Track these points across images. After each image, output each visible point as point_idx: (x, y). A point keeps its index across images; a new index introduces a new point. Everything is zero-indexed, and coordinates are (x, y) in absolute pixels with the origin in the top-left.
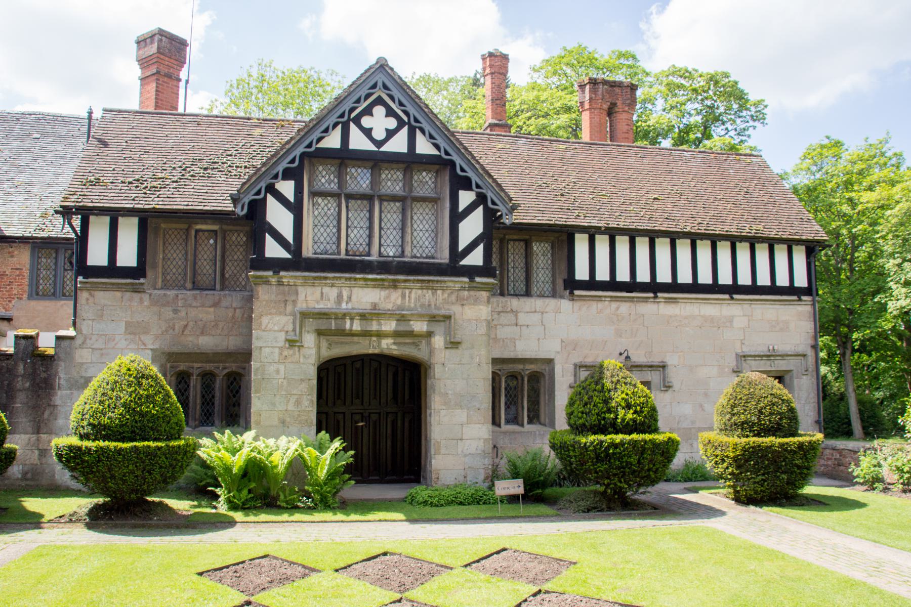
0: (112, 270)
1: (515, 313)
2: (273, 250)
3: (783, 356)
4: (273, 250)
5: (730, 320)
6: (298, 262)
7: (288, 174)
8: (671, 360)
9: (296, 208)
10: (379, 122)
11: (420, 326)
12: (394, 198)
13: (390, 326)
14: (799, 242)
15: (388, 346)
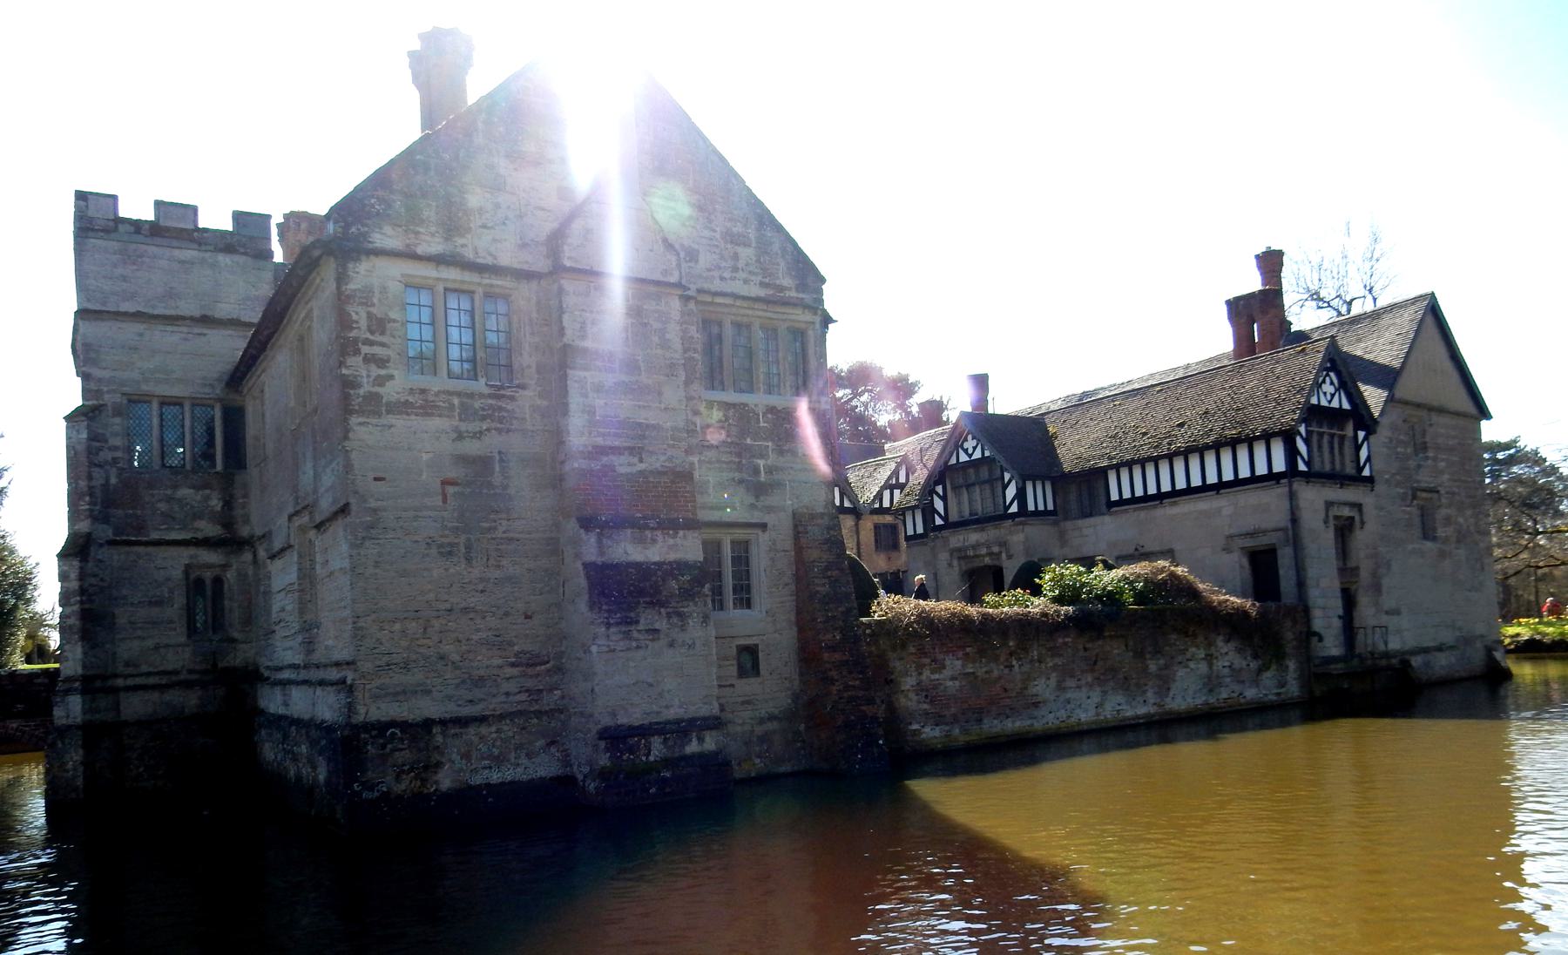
0: (916, 536)
1: (1080, 529)
2: (939, 521)
3: (1265, 532)
4: (939, 521)
5: (1219, 510)
6: (949, 525)
7: (937, 483)
8: (1177, 547)
9: (944, 498)
10: (970, 444)
11: (996, 549)
12: (985, 482)
13: (984, 551)
14: (1275, 435)
15: (987, 560)
